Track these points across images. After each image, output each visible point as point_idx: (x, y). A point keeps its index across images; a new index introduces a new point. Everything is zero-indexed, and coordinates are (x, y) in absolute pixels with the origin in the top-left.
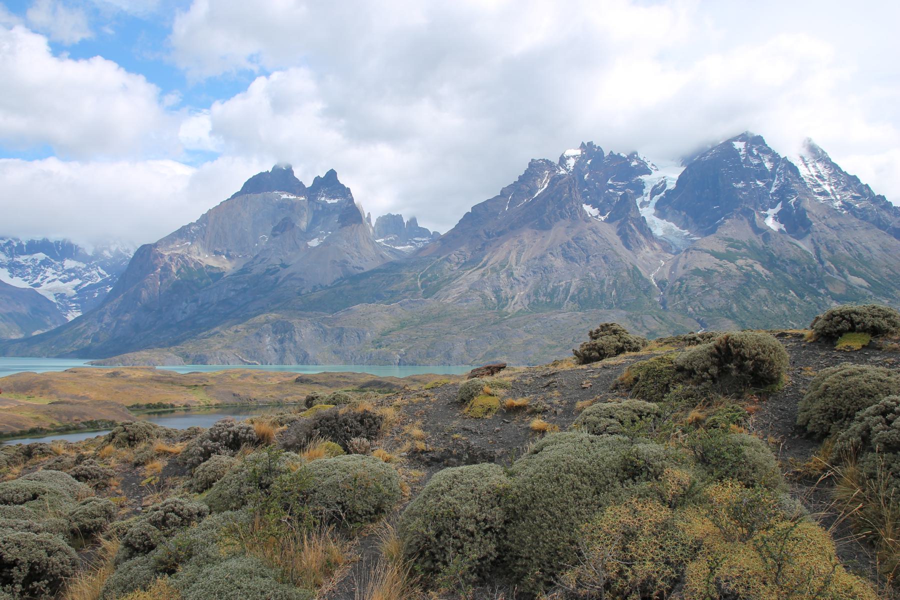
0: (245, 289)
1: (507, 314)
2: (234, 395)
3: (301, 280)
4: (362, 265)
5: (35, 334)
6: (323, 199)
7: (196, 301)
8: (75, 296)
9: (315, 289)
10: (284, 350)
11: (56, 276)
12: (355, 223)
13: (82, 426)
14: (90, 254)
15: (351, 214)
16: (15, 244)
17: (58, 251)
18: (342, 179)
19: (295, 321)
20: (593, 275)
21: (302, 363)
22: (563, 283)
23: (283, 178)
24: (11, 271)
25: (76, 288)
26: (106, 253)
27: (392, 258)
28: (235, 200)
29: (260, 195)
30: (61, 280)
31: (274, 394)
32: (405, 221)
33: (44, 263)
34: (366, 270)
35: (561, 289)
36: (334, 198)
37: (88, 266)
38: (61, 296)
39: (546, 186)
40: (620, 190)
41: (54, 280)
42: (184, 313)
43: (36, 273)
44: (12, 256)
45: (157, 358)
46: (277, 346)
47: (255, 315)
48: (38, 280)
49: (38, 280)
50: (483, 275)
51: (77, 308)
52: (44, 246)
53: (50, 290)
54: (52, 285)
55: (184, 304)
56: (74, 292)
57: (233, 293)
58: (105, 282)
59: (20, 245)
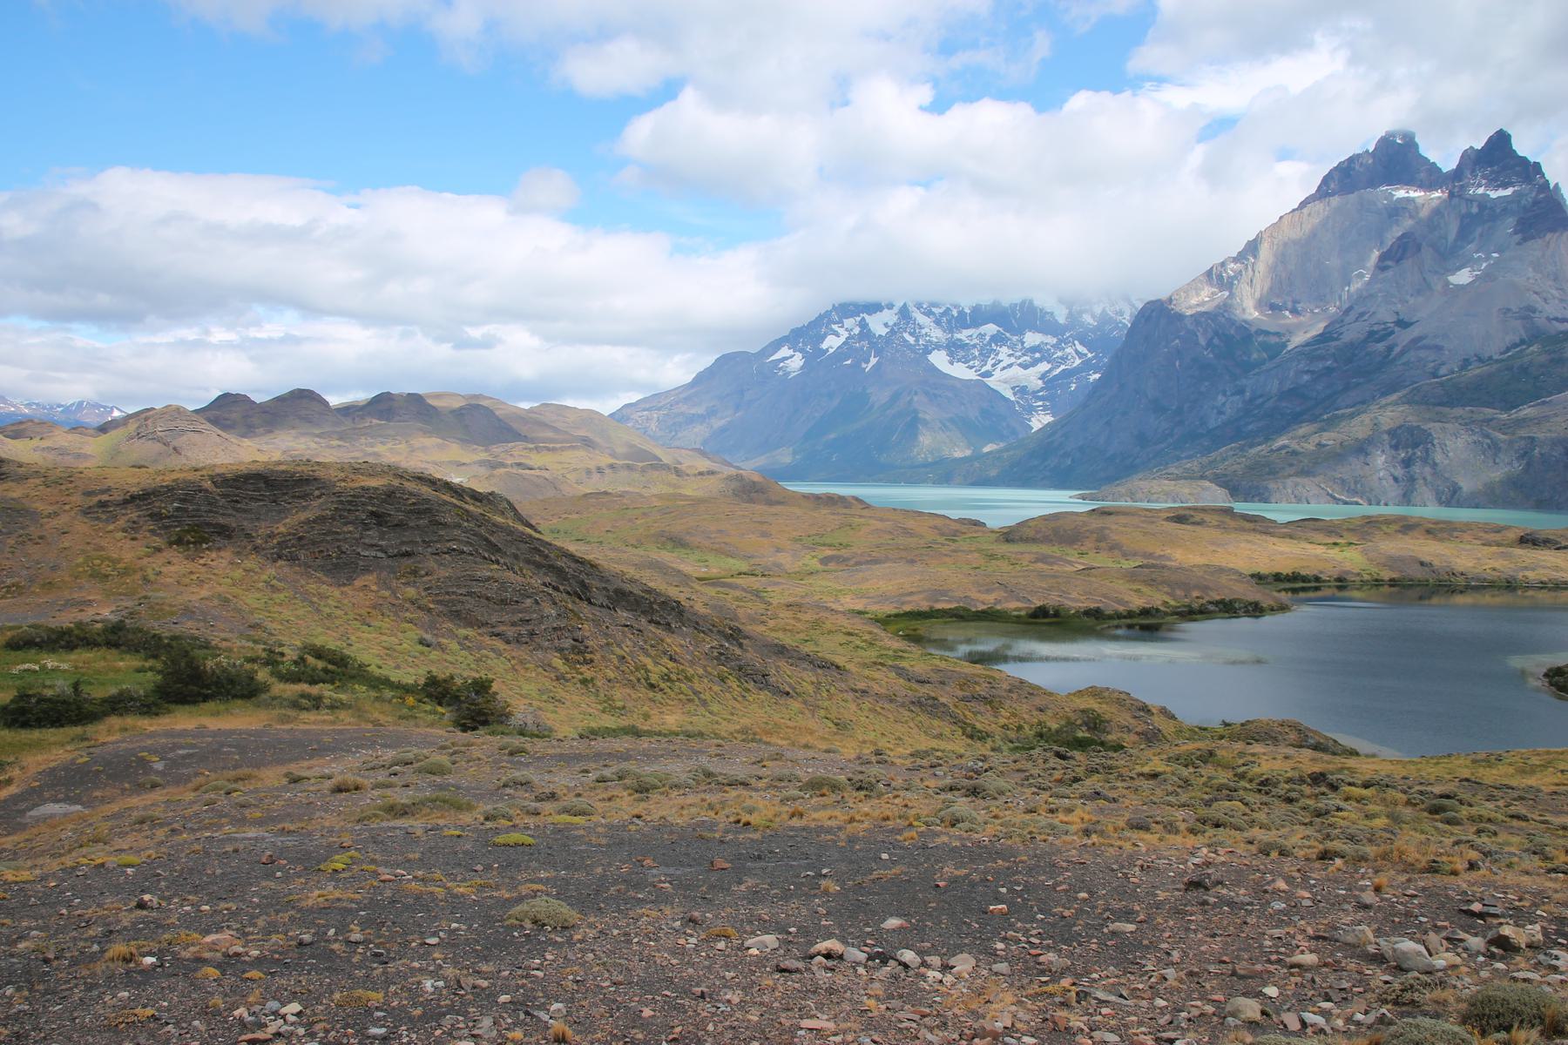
0: (1329, 370)
2: (1422, 564)
3: (1439, 348)
5: (986, 450)
6: (1481, 191)
7: (1241, 392)
8: (1042, 389)
9: (1465, 364)
10: (1412, 479)
11: (1013, 360)
13: (1211, 608)
14: (1062, 320)
16: (955, 313)
17: (1013, 320)
18: (1523, 146)
19: (1434, 427)
21: (1448, 504)
23: (1396, 159)
24: (951, 354)
25: (1042, 377)
26: (1088, 319)
28: (1305, 211)
31: (1497, 565)
33: (997, 339)
36: (1505, 186)
37: (1060, 342)
38: (1021, 390)
41: (1010, 366)
42: (1220, 413)
43: (984, 356)
44: (951, 332)
45: (1187, 491)
46: (1399, 472)
47: (1352, 416)
48: (988, 367)
49: (988, 367)
51: (1045, 408)
52: (998, 315)
53: (1005, 382)
54: (1009, 374)
55: (1220, 398)
57: (1306, 377)
58: (1087, 366)
59: (961, 313)
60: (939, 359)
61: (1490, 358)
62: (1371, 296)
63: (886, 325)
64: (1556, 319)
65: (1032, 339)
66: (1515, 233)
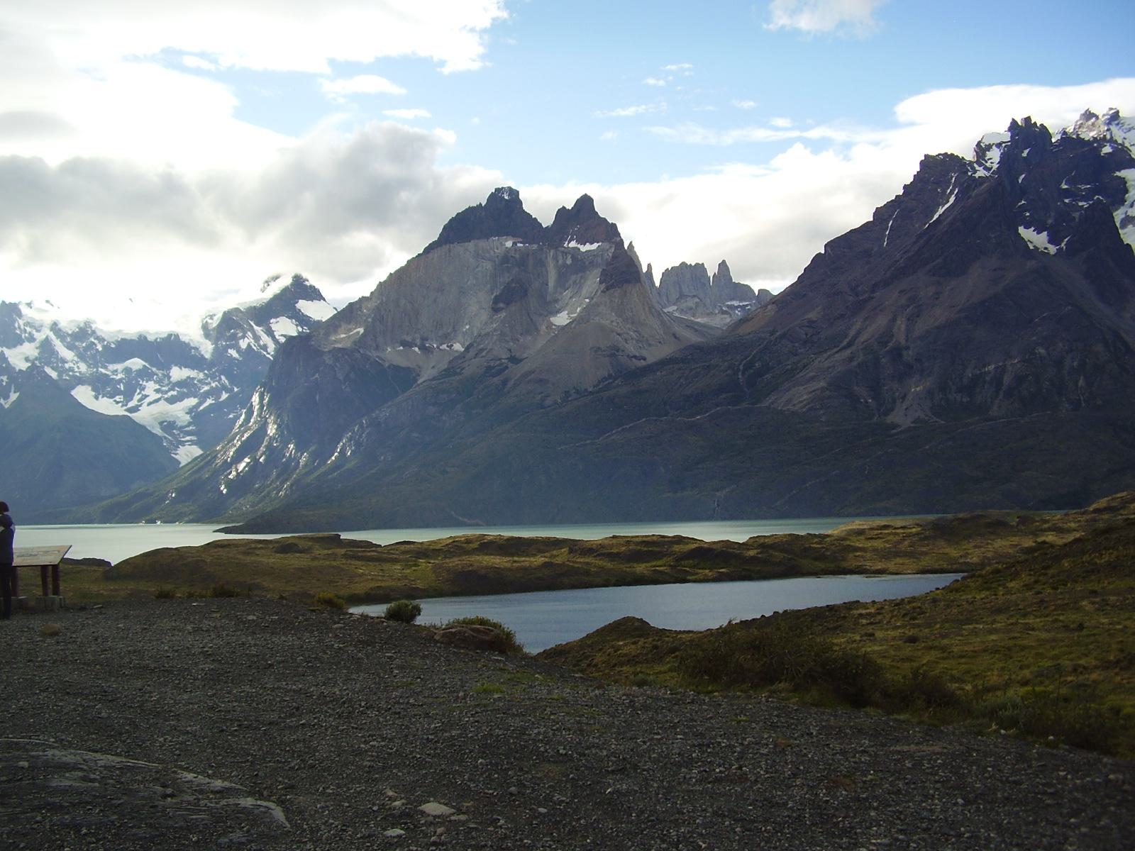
1: (895, 426)
4: (644, 353)
6: (573, 244)
8: (190, 424)
11: (159, 395)
12: (628, 281)
15: (622, 268)
16: (100, 348)
20: (1042, 351)
22: (991, 367)
25: (190, 411)
26: (233, 353)
27: (695, 339)
28: (431, 255)
29: (471, 245)
30: (167, 400)
32: (710, 274)
33: (145, 374)
34: (651, 359)
35: (988, 378)
38: (168, 426)
39: (952, 199)
40: (1084, 199)
41: (157, 401)
50: (851, 359)
51: (193, 443)
56: (188, 417)
60: (83, 395)
61: (586, 390)
62: (487, 334)
63: (27, 359)
64: (635, 357)
65: (178, 373)
66: (601, 282)
